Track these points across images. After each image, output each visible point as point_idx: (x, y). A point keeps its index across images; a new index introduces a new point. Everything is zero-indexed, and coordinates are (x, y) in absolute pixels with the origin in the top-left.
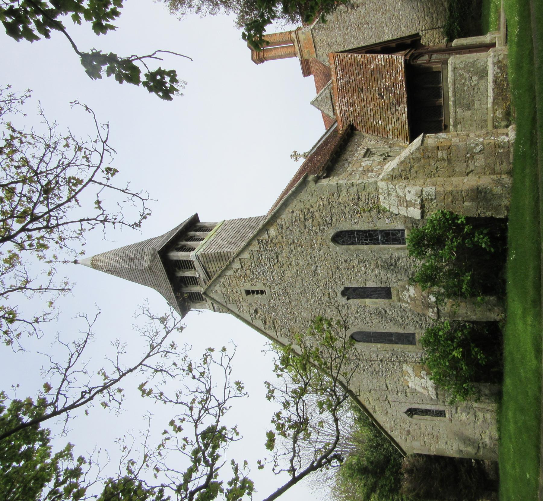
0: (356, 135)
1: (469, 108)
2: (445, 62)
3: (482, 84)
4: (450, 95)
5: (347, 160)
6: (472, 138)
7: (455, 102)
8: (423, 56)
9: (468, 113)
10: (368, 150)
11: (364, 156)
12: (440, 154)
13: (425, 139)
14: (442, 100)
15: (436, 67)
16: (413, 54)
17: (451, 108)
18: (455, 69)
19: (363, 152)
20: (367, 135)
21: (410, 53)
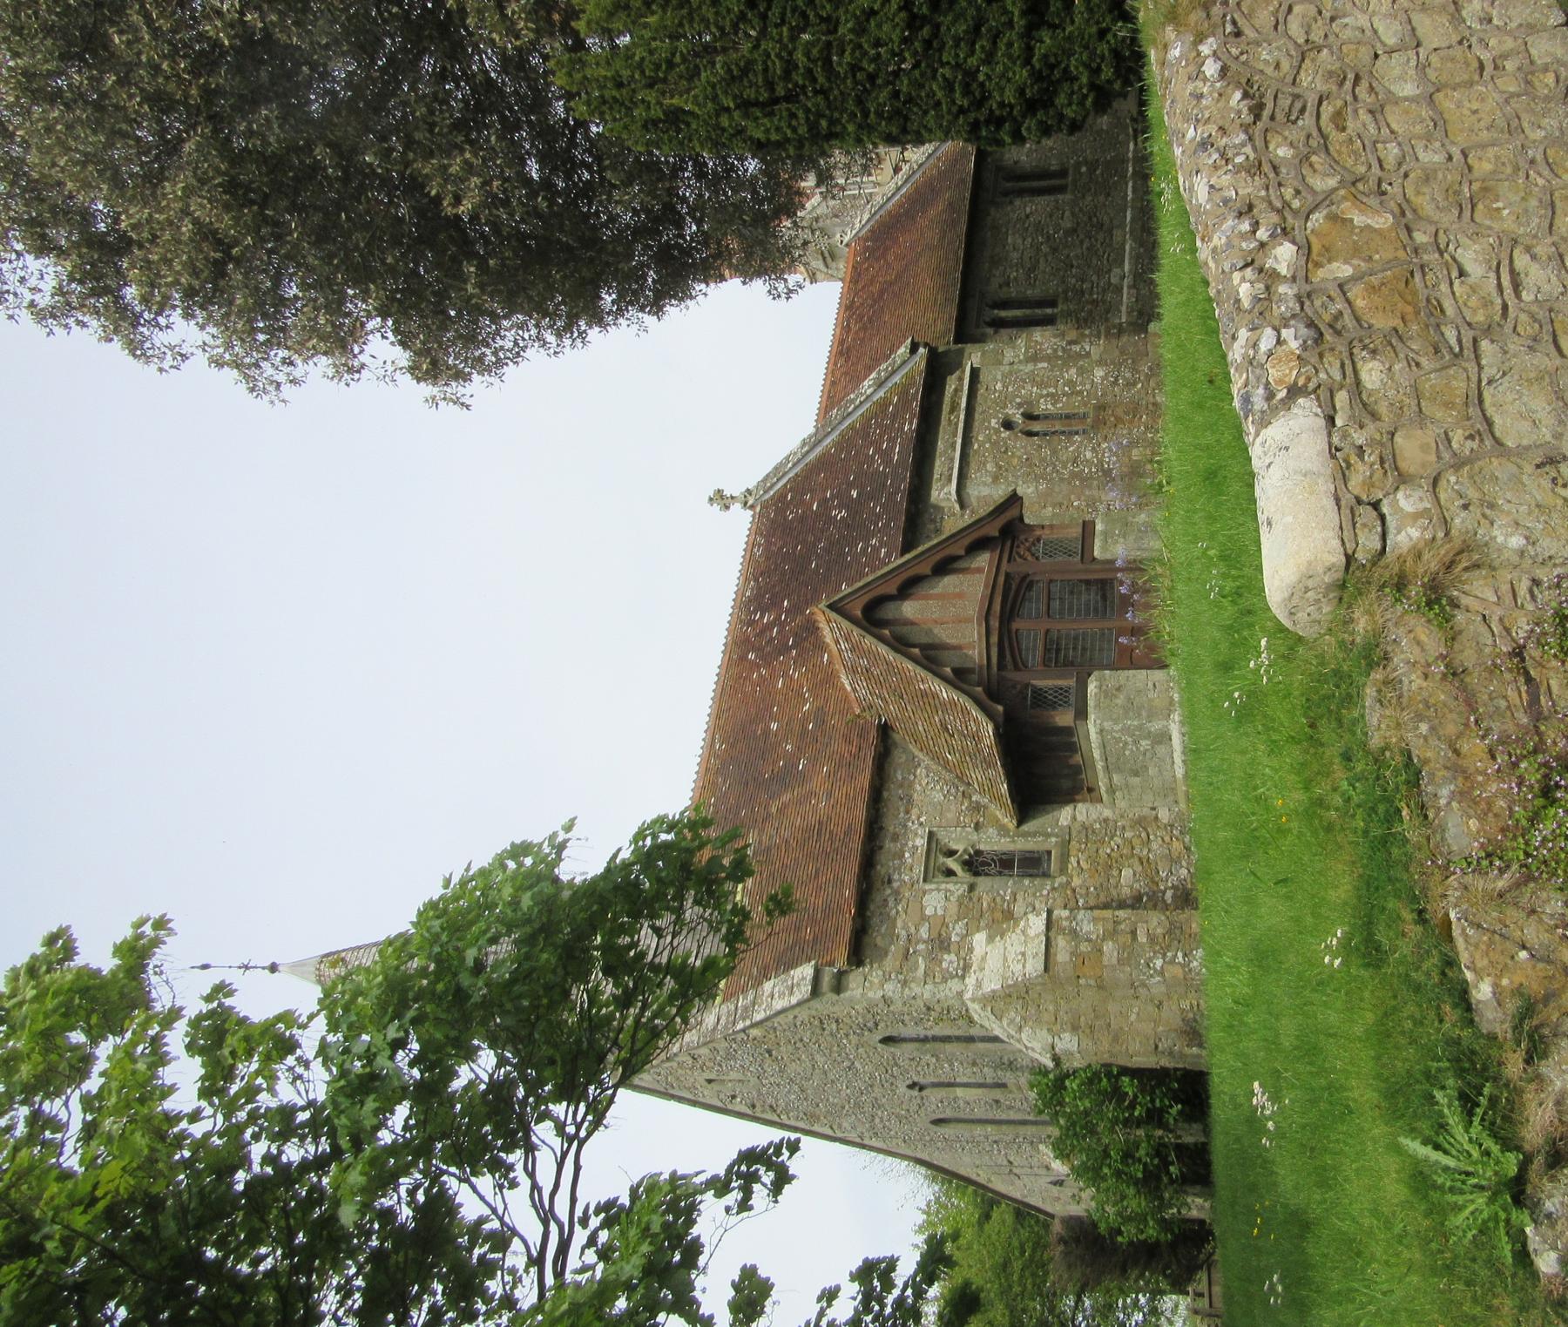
0: (895, 744)
1: (1136, 774)
2: (1082, 714)
3: (1161, 750)
4: (1097, 754)
5: (890, 881)
6: (1141, 945)
7: (1107, 768)
8: (1030, 585)
9: (1137, 780)
10: (931, 834)
11: (925, 880)
12: (1082, 981)
13: (1052, 934)
14: (1077, 759)
15: (1064, 718)
16: (1008, 575)
17: (1101, 774)
18: (1101, 731)
19: (921, 842)
20: (921, 755)
21: (1001, 579)
